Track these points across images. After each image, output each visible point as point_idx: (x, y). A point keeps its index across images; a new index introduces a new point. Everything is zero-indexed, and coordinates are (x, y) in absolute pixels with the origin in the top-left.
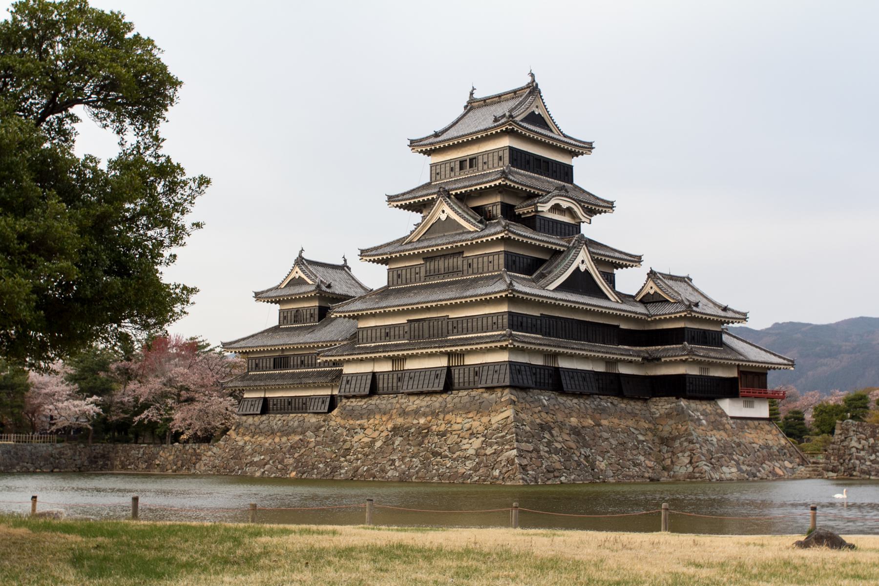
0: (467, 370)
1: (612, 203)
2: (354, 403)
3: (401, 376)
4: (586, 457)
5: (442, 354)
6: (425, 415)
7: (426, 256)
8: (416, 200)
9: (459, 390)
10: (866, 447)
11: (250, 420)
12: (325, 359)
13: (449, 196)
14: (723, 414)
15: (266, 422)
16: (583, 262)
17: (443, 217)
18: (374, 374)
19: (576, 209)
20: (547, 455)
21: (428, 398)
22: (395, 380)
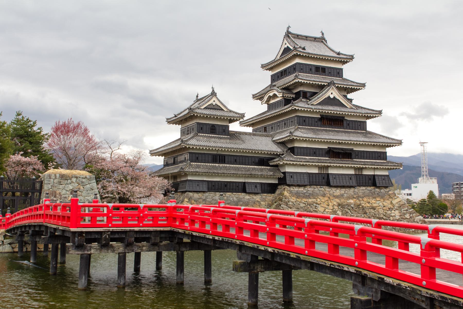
0: (364, 177)
2: (296, 189)
5: (351, 168)
6: (349, 198)
7: (322, 114)
8: (314, 83)
9: (360, 186)
11: (196, 195)
12: (285, 162)
15: (211, 197)
17: (332, 96)
21: (344, 189)
22: (320, 178)
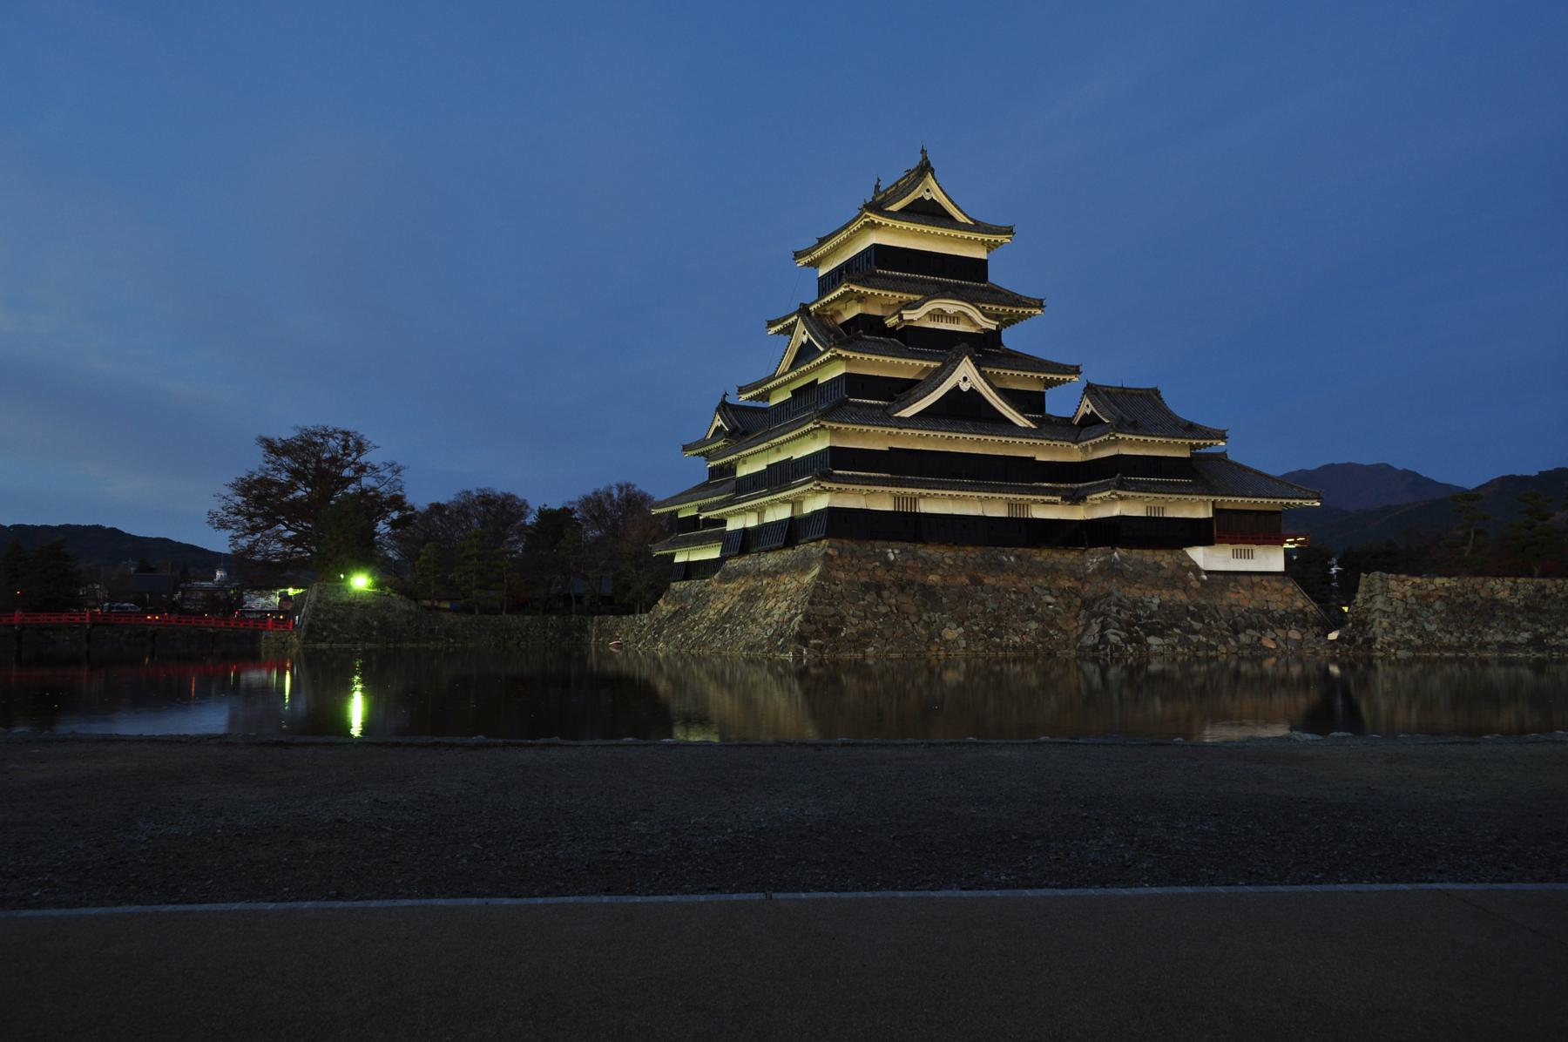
1: (1041, 301)
3: (763, 529)
4: (928, 625)
10: (1400, 610)
13: (809, 313)
14: (1196, 569)
16: (965, 379)
17: (805, 339)
18: (745, 530)
19: (970, 313)
20: (855, 621)
